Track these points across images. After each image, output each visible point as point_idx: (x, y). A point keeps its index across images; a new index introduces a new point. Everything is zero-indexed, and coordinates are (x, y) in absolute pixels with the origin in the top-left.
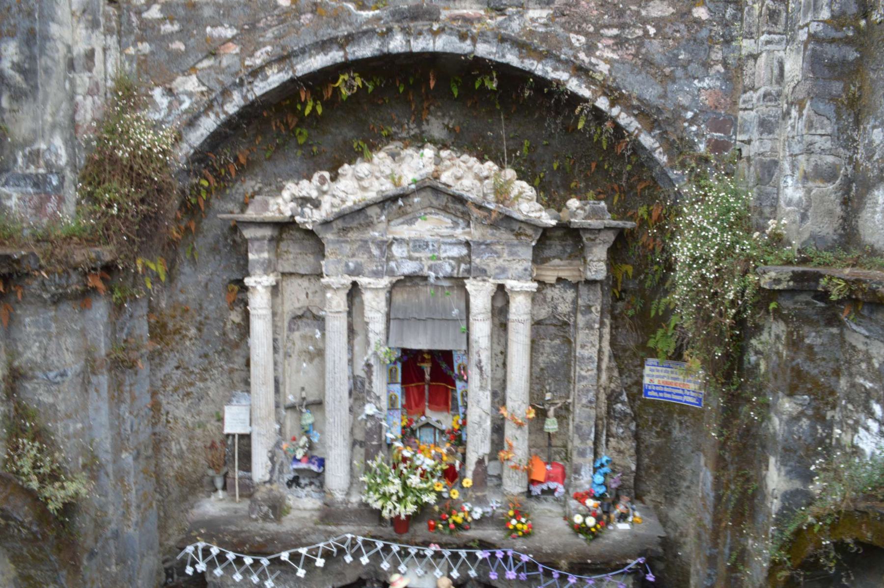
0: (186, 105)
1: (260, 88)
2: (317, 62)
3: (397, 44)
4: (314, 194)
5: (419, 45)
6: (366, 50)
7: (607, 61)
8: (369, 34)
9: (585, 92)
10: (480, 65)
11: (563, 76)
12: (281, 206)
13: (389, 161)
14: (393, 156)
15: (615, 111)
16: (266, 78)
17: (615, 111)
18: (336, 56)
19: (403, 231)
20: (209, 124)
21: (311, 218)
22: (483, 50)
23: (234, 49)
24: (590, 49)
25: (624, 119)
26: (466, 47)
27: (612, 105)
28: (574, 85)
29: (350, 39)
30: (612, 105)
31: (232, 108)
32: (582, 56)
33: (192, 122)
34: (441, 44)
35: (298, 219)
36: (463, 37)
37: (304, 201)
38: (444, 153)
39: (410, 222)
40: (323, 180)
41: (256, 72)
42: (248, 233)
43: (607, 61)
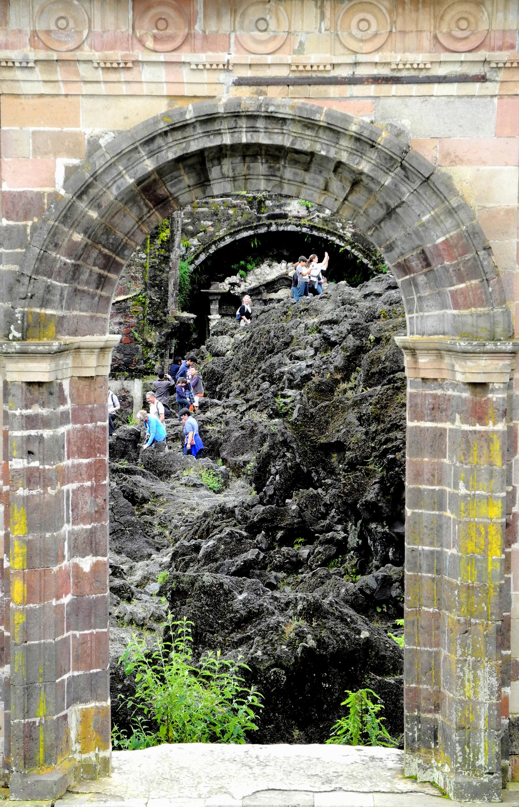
0: (193, 249)
1: (222, 244)
2: (245, 234)
3: (273, 228)
4: (238, 282)
5: (281, 229)
6: (263, 230)
7: (350, 232)
8: (263, 225)
9: (343, 245)
10: (304, 234)
11: (333, 238)
12: (224, 286)
13: (268, 268)
14: (270, 266)
15: (353, 251)
16: (224, 240)
17: (353, 251)
18: (251, 232)
19: (273, 296)
20: (203, 257)
21: (238, 290)
22: (304, 230)
23: (212, 229)
24: (343, 228)
25: (356, 253)
26: (299, 229)
27: (352, 248)
28: (337, 242)
29: (256, 227)
30: (352, 248)
31: (211, 251)
32: (341, 231)
33: (197, 257)
34: (290, 228)
35: (232, 292)
36: (297, 226)
37: (233, 284)
38: (290, 264)
39: (276, 292)
40: (241, 276)
41: (222, 239)
42: (211, 298)
43: (350, 232)
